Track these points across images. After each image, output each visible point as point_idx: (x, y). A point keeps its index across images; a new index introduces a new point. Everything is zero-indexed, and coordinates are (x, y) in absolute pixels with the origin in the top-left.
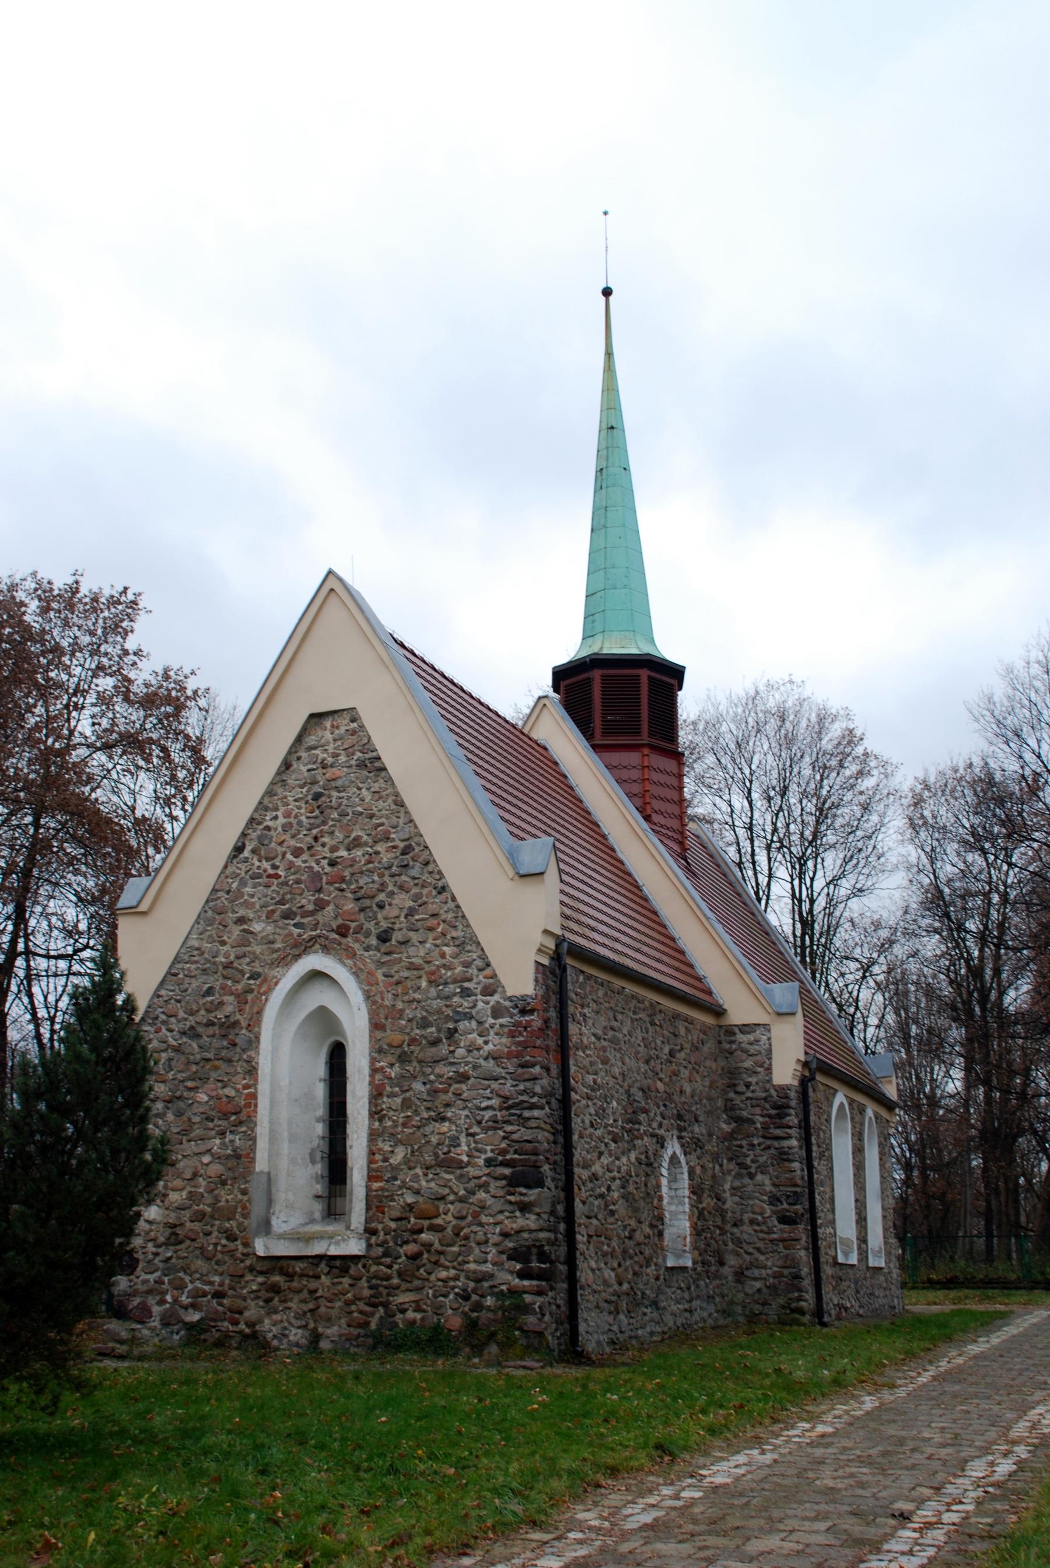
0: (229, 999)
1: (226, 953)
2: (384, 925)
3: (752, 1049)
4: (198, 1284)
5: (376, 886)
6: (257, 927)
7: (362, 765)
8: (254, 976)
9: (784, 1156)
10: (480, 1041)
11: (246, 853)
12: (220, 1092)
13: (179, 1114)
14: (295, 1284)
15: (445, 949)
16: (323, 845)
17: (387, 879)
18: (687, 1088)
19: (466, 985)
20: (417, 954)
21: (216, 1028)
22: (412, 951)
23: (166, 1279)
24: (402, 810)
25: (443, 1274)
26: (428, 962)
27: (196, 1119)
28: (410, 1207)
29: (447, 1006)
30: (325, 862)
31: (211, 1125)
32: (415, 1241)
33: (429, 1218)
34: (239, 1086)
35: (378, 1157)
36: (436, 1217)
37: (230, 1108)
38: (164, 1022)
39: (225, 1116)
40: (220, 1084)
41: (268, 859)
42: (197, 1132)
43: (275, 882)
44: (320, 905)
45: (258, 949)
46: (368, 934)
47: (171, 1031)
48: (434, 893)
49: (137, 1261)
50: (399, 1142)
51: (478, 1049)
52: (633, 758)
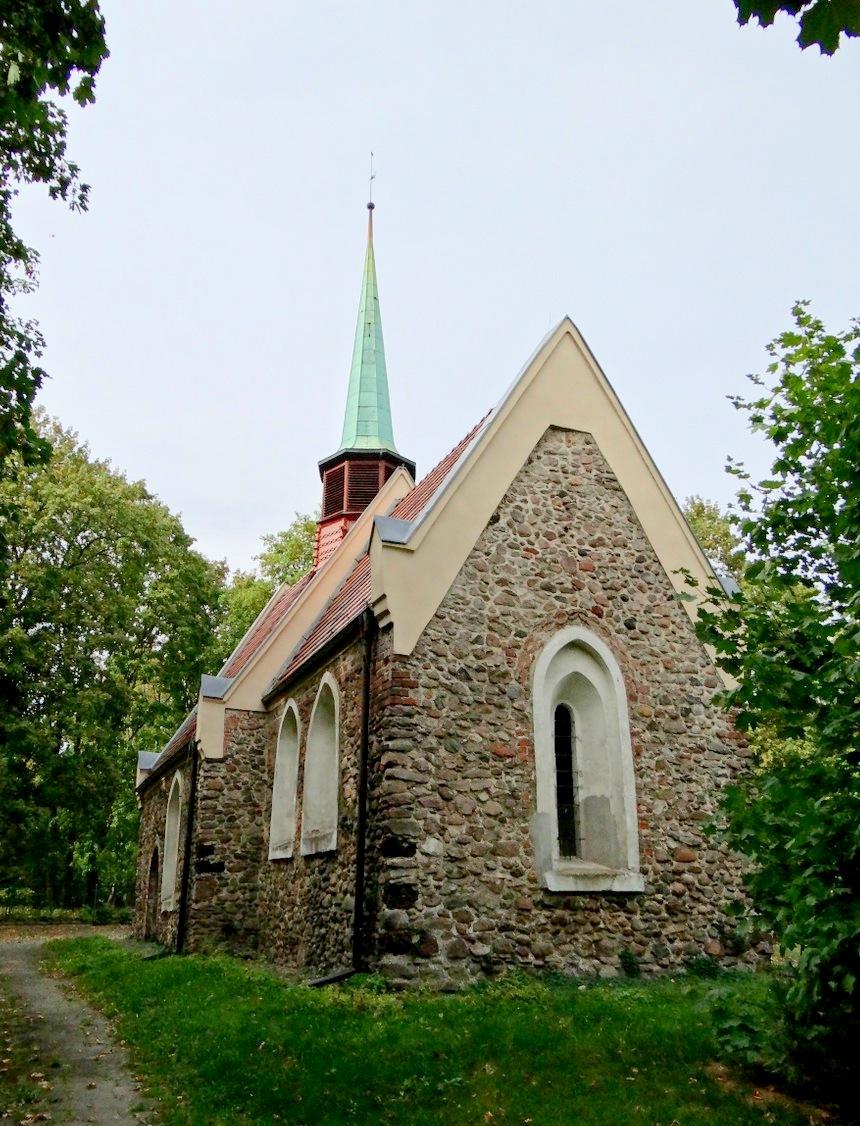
0: (497, 650)
1: (490, 608)
2: (629, 616)
4: (484, 918)
5: (621, 582)
6: (518, 591)
8: (520, 634)
10: (709, 722)
11: (502, 522)
12: (494, 735)
13: (453, 750)
14: (579, 917)
15: (674, 644)
16: (572, 536)
17: (627, 578)
19: (694, 676)
20: (658, 643)
21: (486, 674)
23: (450, 913)
24: (635, 527)
25: (703, 908)
26: (664, 652)
27: (471, 757)
28: (672, 852)
29: (682, 690)
30: (576, 551)
31: (487, 765)
32: (679, 881)
33: (689, 862)
34: (513, 732)
35: (643, 808)
36: (693, 861)
37: (504, 751)
38: (432, 660)
39: (500, 757)
40: (492, 727)
41: (522, 535)
42: (473, 770)
43: (534, 556)
44: (577, 587)
45: (522, 612)
46: (618, 620)
47: (441, 669)
48: (665, 599)
49: (415, 894)
50: (658, 797)
51: (709, 728)
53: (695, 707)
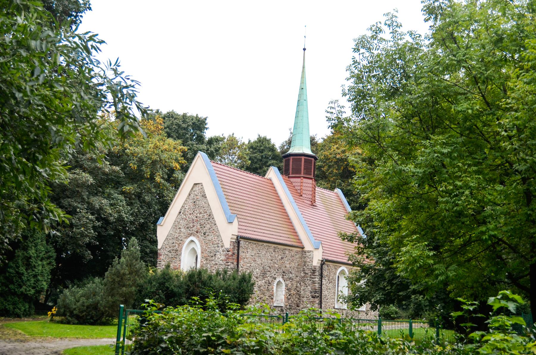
3: (310, 257)
6: (182, 230)
7: (203, 196)
9: (314, 282)
18: (288, 266)
22: (209, 237)
44: (194, 226)
45: (182, 235)
52: (298, 180)
53: (217, 253)
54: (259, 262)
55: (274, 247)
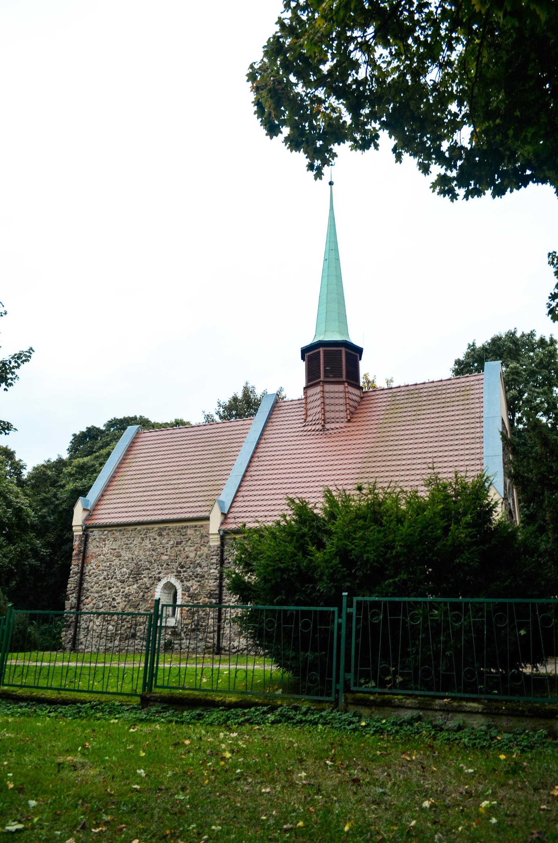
18: (192, 555)
54: (126, 555)
55: (160, 529)
